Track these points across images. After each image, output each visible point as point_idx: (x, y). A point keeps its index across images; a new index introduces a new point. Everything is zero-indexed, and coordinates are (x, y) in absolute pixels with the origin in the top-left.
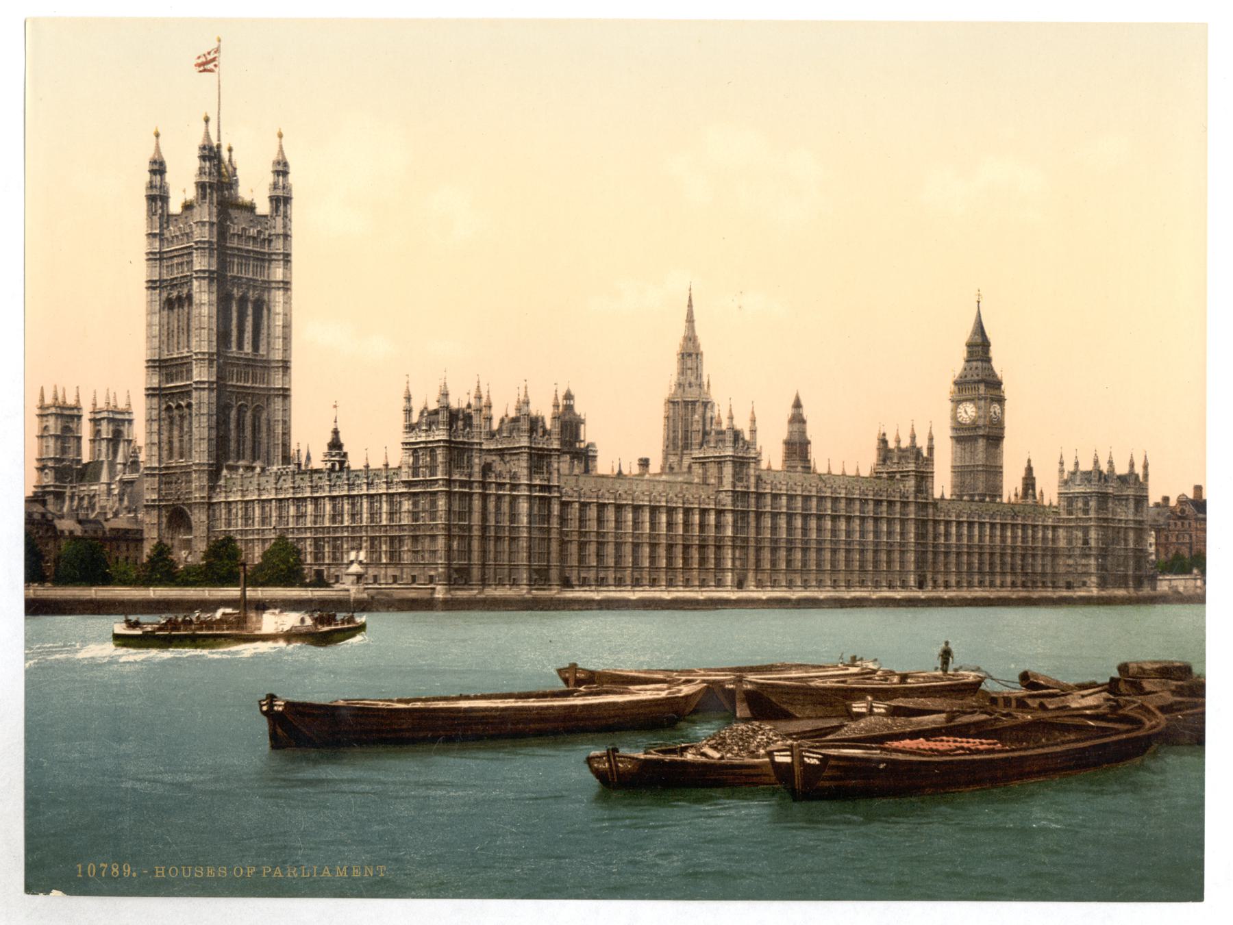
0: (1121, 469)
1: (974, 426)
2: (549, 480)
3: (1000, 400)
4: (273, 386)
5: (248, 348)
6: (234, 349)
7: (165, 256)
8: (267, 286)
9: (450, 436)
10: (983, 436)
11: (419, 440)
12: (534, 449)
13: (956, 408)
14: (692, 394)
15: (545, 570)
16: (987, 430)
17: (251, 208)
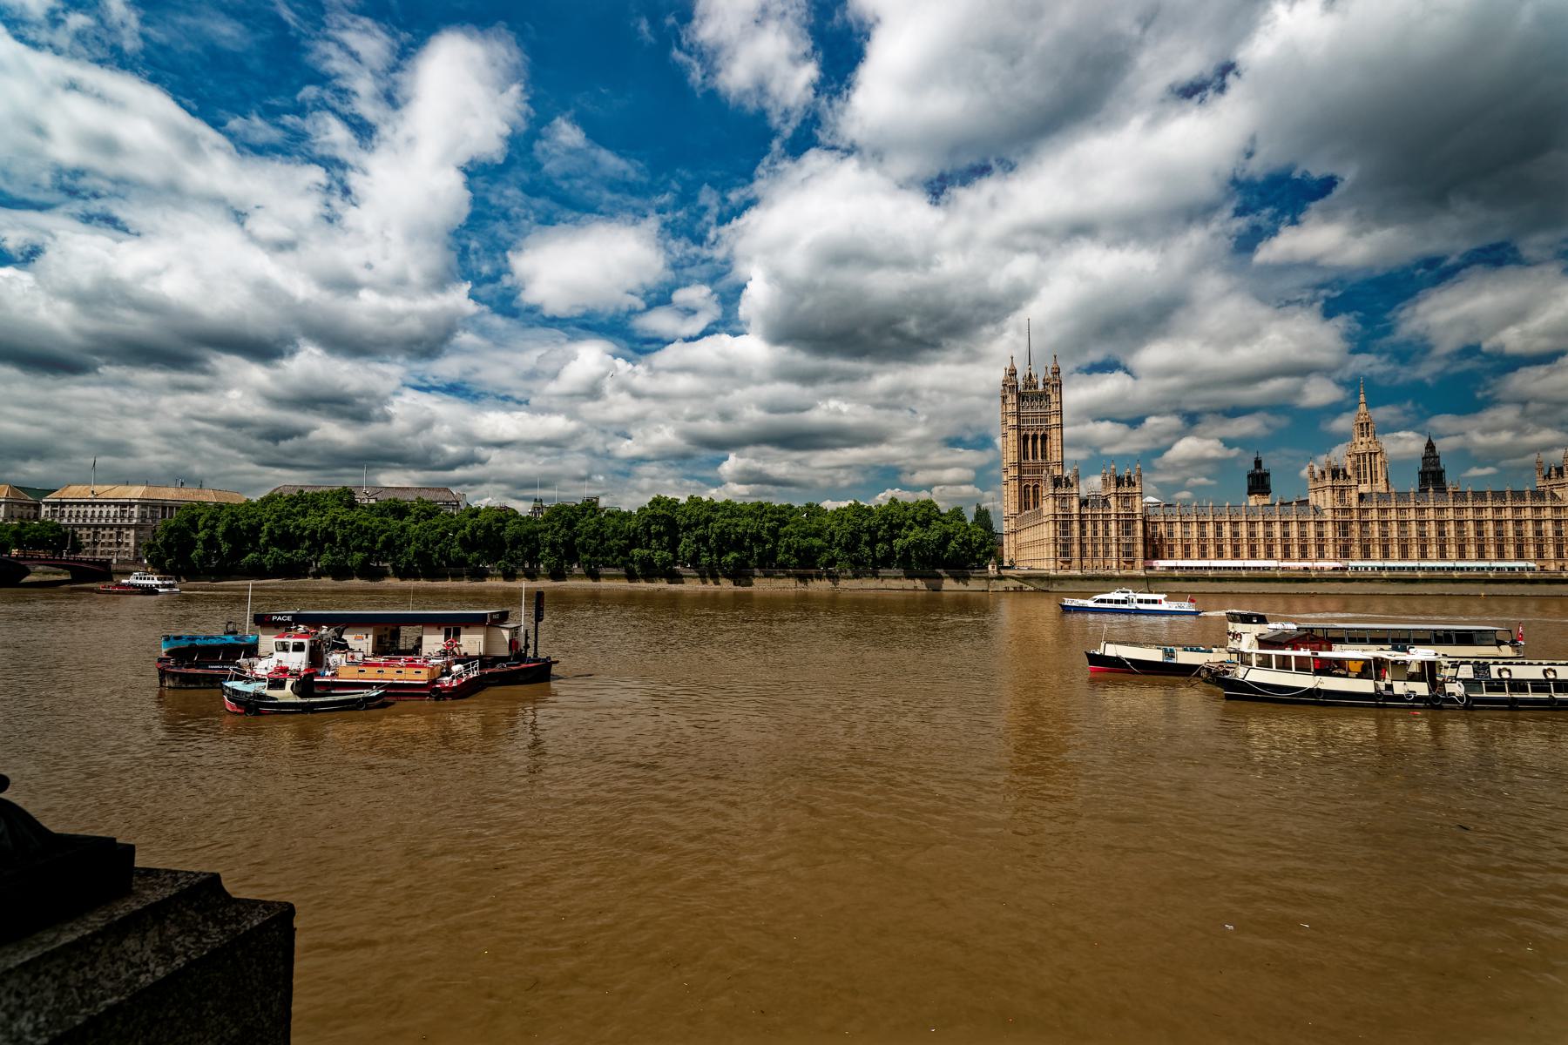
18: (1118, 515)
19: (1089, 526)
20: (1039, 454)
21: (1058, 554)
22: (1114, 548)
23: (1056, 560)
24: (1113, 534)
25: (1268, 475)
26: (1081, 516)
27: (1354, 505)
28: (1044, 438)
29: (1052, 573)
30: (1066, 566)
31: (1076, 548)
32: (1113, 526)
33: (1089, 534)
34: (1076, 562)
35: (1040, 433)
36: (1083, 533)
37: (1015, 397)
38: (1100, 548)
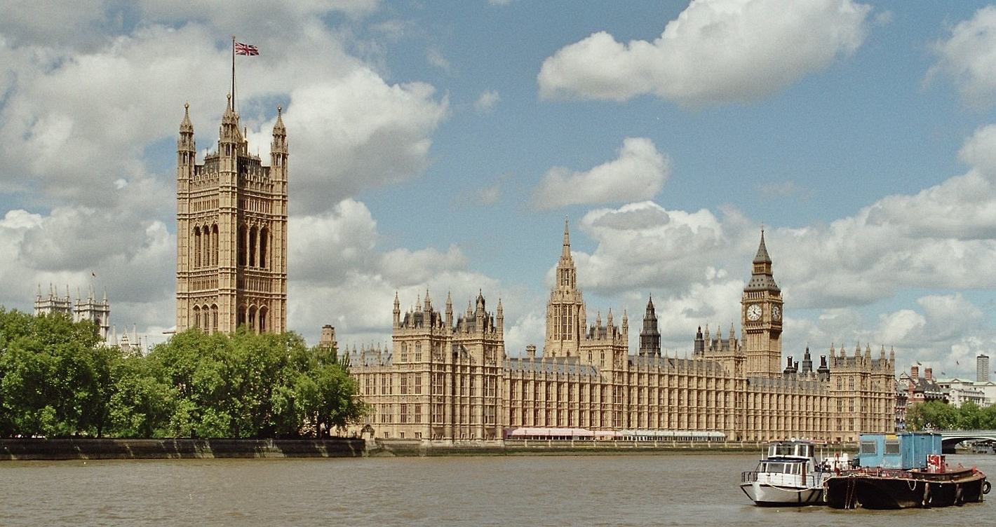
0: (875, 353)
1: (760, 322)
2: (495, 364)
3: (779, 305)
4: (274, 293)
5: (258, 265)
6: (248, 265)
7: (193, 196)
8: (270, 220)
9: (432, 332)
10: (767, 330)
11: (406, 334)
12: (487, 341)
13: (747, 308)
14: (569, 299)
15: (442, 428)
16: (771, 325)
17: (257, 162)
18: (483, 367)
22: (479, 411)
24: (479, 393)
26: (454, 367)
29: (426, 444)
31: (448, 410)
32: (478, 382)
33: (458, 390)
34: (448, 429)
35: (260, 226)
38: (467, 411)
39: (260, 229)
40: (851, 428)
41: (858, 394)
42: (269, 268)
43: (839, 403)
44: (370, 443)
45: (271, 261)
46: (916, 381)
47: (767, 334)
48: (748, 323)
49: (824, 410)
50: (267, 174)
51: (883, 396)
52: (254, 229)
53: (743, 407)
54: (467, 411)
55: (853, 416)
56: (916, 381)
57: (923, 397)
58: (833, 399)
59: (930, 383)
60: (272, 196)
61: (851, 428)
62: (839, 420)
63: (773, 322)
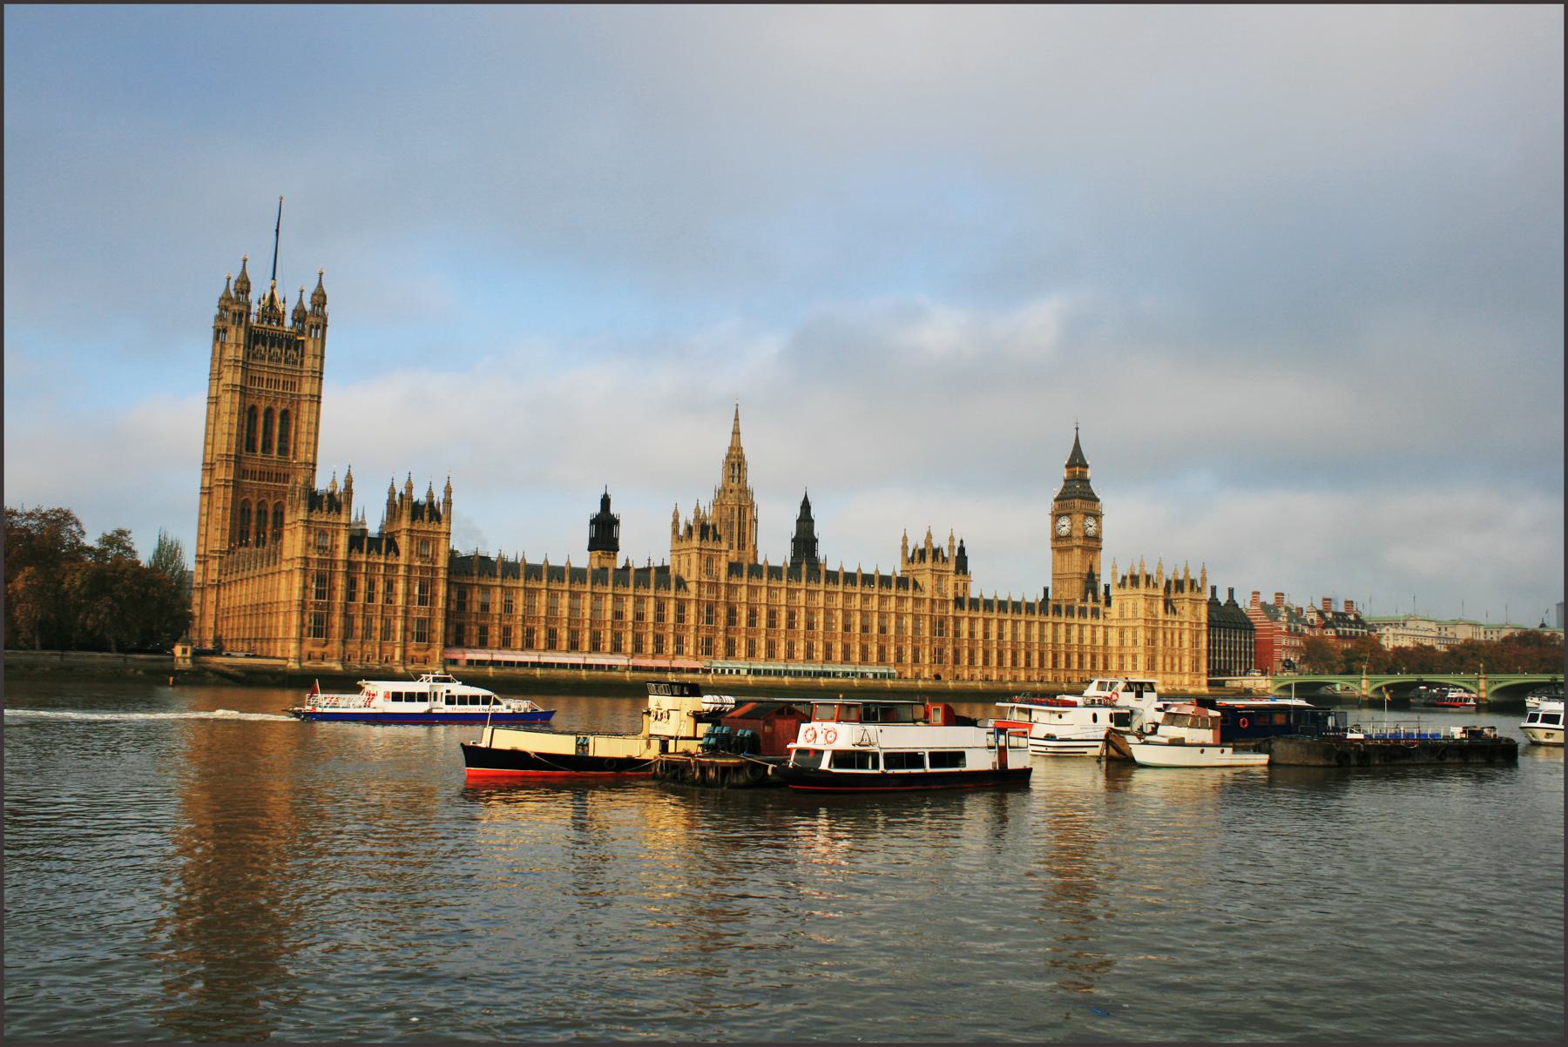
1: (1069, 537)
3: (1097, 516)
10: (1078, 547)
18: (409, 568)
19: (362, 584)
20: (276, 445)
21: (305, 631)
22: (399, 624)
23: (301, 641)
24: (400, 600)
25: (617, 522)
26: (351, 565)
27: (722, 580)
28: (285, 415)
29: (293, 665)
30: (318, 651)
33: (361, 597)
35: (279, 408)
36: (351, 596)
37: (242, 333)
39: (278, 412)
40: (1134, 666)
41: (1141, 622)
42: (291, 456)
43: (1121, 634)
44: (180, 661)
45: (295, 448)
46: (1329, 615)
47: (1077, 552)
48: (1057, 538)
49: (1100, 642)
50: (296, 349)
51: (1186, 625)
52: (269, 412)
53: (947, 635)
54: (377, 623)
55: (1136, 651)
56: (1329, 615)
57: (1333, 634)
58: (1115, 630)
59: (1352, 618)
60: (301, 372)
61: (1134, 666)
62: (1121, 657)
63: (1086, 537)
